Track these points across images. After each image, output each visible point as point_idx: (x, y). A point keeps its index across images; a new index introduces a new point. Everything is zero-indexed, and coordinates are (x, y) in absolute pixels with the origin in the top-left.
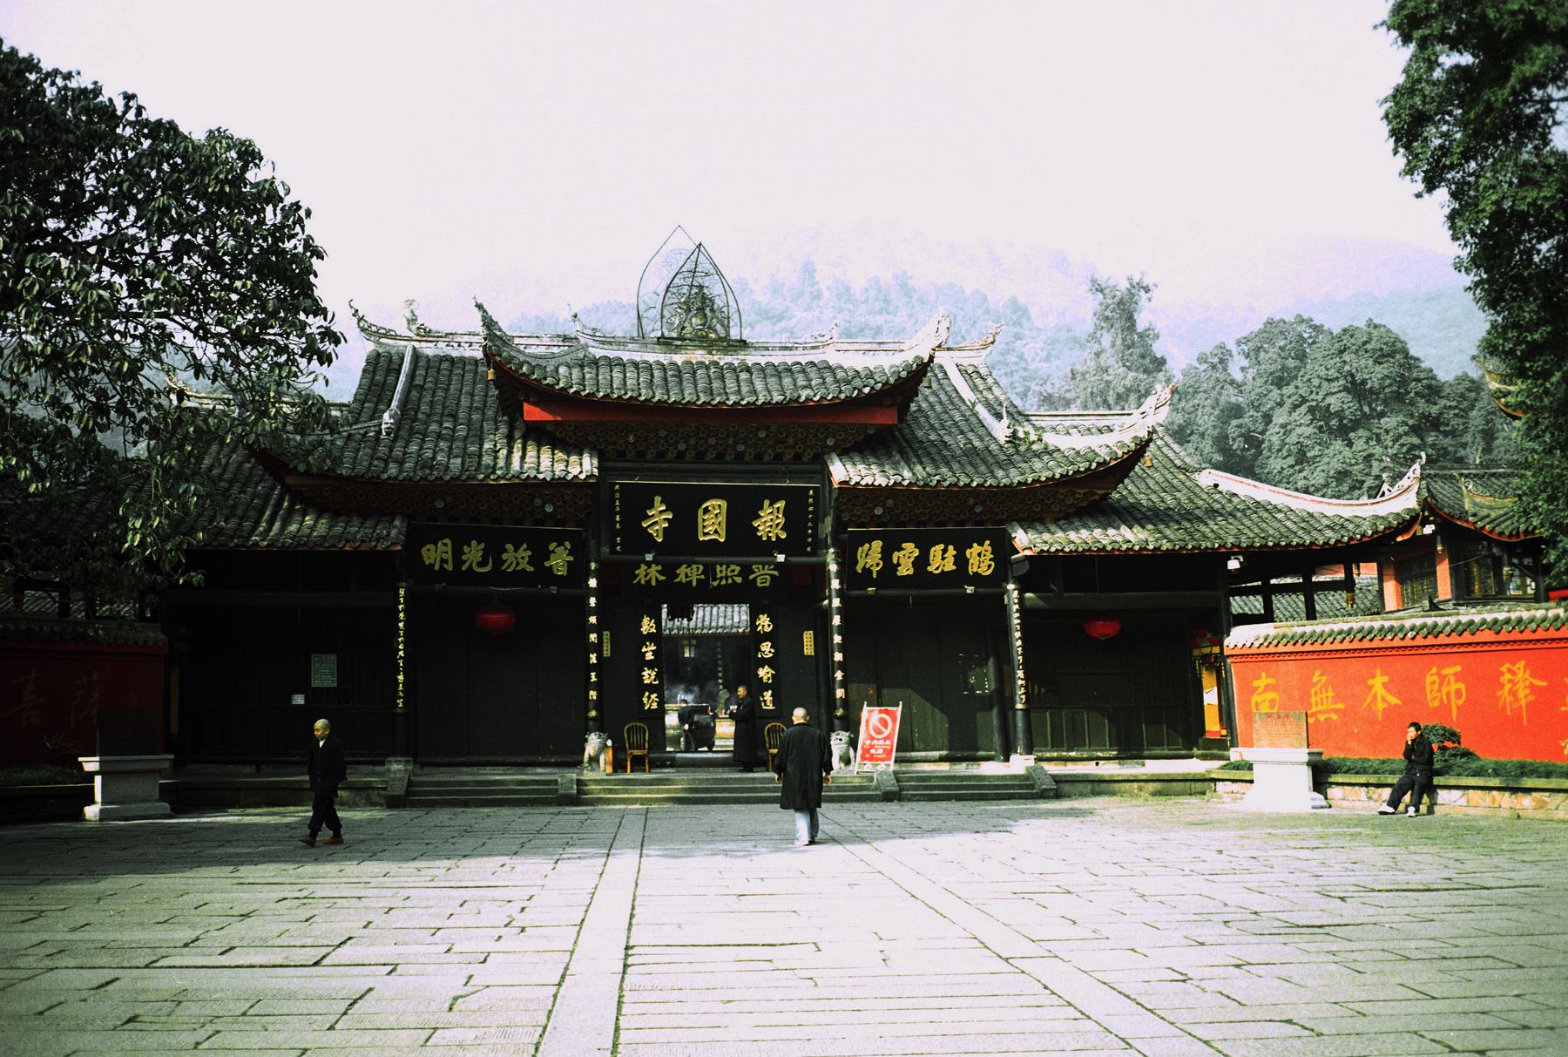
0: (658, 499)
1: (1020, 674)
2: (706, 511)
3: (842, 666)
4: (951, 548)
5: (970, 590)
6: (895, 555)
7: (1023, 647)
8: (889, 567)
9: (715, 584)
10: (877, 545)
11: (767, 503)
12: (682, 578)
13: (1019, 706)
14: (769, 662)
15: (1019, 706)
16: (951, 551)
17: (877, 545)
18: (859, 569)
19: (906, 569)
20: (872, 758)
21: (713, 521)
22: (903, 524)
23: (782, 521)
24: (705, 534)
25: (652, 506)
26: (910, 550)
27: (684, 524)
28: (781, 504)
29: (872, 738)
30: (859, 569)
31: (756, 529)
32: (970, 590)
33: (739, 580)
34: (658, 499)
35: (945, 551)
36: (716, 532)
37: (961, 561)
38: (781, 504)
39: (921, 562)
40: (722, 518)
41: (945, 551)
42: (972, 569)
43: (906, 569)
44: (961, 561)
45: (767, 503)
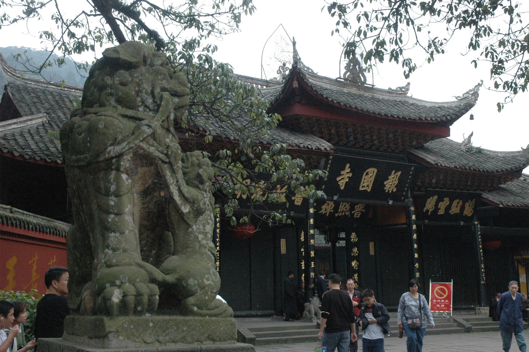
0: (348, 165)
1: (483, 266)
2: (367, 174)
3: (418, 260)
4: (461, 201)
5: (462, 223)
6: (440, 203)
7: (483, 252)
8: (437, 209)
9: (336, 215)
10: (436, 197)
11: (394, 172)
12: (323, 211)
13: (482, 282)
14: (357, 258)
15: (482, 282)
16: (461, 203)
17: (436, 197)
18: (424, 210)
19: (441, 212)
20: (438, 309)
21: (367, 181)
22: (449, 189)
23: (396, 182)
24: (363, 187)
25: (344, 169)
26: (447, 200)
27: (355, 180)
28: (399, 173)
29: (437, 299)
30: (424, 210)
31: (385, 186)
32: (462, 223)
33: (348, 213)
34: (348, 165)
35: (458, 203)
36: (368, 186)
37: (463, 208)
38: (399, 173)
39: (448, 208)
40: (373, 179)
41: (458, 203)
42: (465, 213)
43: (441, 212)
44: (463, 208)
45: (394, 172)
